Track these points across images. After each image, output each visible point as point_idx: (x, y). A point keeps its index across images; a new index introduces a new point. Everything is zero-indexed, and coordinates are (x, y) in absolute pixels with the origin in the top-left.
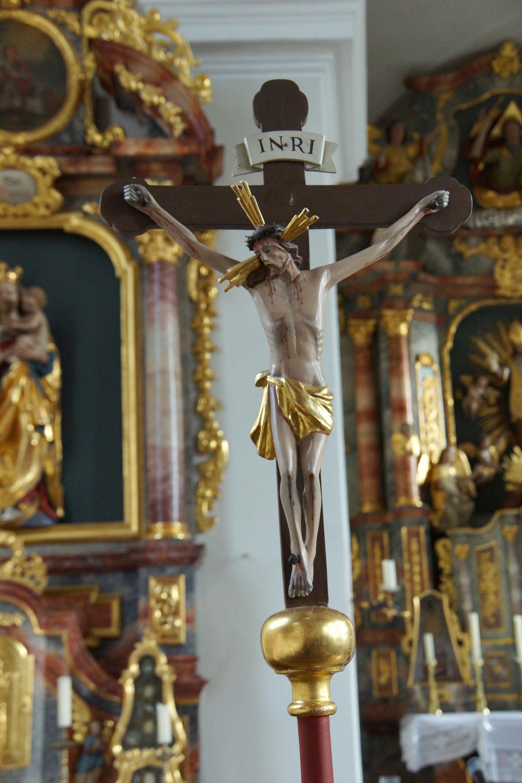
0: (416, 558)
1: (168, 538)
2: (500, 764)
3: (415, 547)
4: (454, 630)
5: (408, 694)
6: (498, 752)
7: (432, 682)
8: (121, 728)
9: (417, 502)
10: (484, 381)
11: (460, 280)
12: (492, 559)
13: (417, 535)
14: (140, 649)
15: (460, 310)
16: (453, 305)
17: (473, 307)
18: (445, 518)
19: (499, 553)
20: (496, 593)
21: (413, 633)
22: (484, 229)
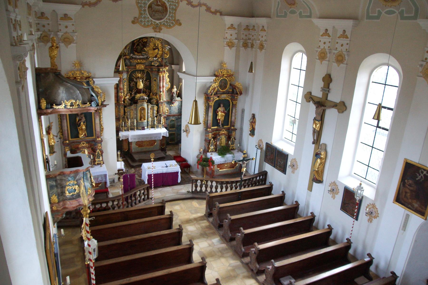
0: (122, 111)
1: (99, 140)
2: (131, 140)
3: (122, 109)
4: (127, 121)
5: (120, 129)
6: (131, 139)
7: (123, 127)
8: (96, 157)
9: (123, 103)
10: (133, 82)
11: (131, 67)
12: (132, 111)
13: (122, 108)
14: (97, 151)
15: (130, 71)
16: (130, 70)
17: (132, 70)
18: (126, 104)
19: (134, 110)
20: (133, 115)
21: (121, 121)
22: (135, 58)
